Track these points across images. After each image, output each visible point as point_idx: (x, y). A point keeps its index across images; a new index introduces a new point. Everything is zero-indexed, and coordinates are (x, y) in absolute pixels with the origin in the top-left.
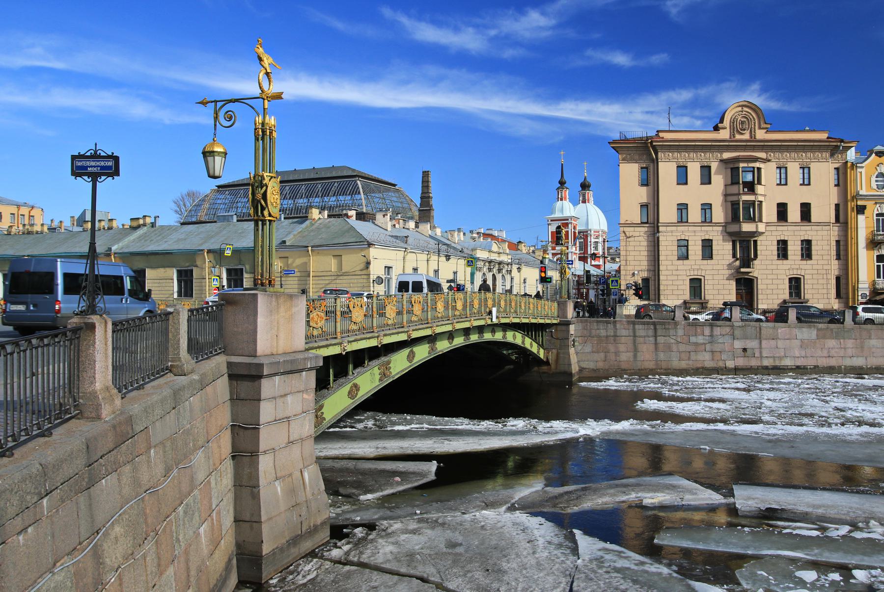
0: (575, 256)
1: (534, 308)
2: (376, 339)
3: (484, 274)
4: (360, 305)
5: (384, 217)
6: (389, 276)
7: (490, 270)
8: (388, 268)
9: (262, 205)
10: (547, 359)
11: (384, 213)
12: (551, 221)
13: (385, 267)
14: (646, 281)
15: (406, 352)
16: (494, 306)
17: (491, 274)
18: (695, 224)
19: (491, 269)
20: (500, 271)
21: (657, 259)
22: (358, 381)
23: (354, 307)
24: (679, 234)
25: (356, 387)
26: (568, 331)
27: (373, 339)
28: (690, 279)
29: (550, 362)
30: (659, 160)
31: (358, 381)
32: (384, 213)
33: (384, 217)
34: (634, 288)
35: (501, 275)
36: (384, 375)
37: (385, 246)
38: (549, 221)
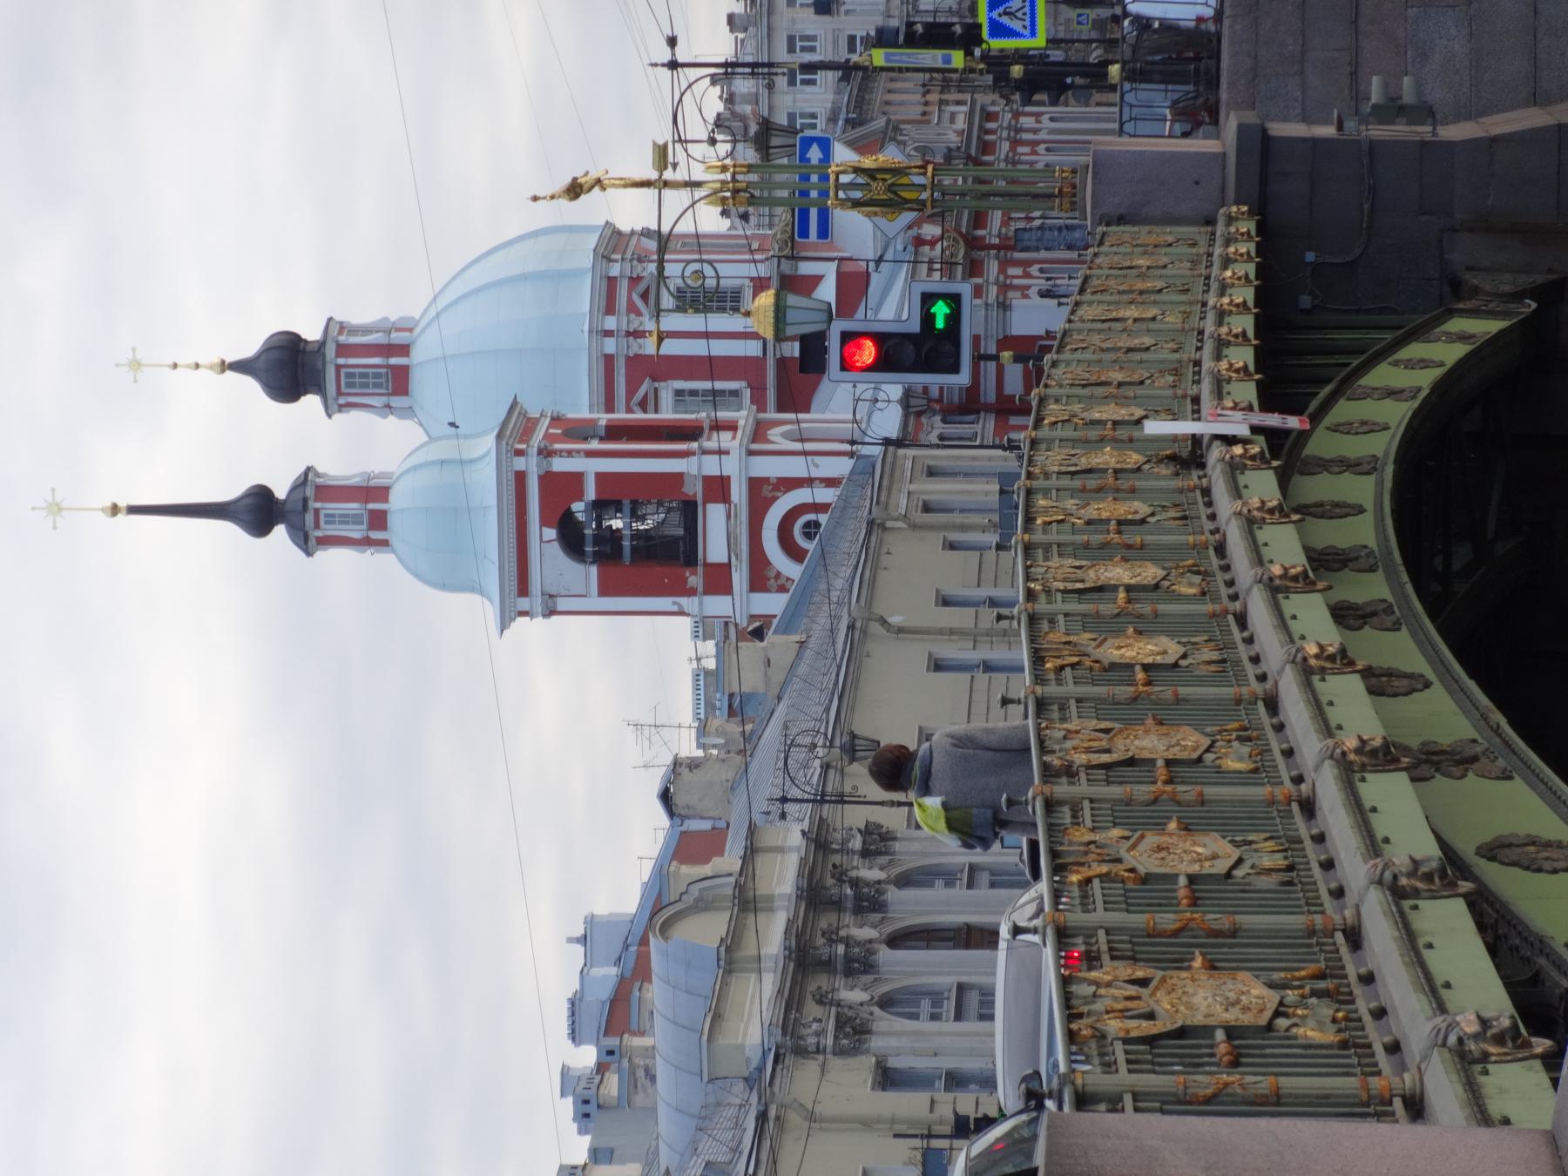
0: (774, 434)
3: (886, 1003)
4: (1132, 990)
7: (859, 965)
10: (1518, 296)
12: (523, 590)
17: (885, 954)
19: (848, 959)
20: (869, 903)
23: (1150, 1016)
29: (1540, 279)
35: (893, 894)
38: (524, 603)
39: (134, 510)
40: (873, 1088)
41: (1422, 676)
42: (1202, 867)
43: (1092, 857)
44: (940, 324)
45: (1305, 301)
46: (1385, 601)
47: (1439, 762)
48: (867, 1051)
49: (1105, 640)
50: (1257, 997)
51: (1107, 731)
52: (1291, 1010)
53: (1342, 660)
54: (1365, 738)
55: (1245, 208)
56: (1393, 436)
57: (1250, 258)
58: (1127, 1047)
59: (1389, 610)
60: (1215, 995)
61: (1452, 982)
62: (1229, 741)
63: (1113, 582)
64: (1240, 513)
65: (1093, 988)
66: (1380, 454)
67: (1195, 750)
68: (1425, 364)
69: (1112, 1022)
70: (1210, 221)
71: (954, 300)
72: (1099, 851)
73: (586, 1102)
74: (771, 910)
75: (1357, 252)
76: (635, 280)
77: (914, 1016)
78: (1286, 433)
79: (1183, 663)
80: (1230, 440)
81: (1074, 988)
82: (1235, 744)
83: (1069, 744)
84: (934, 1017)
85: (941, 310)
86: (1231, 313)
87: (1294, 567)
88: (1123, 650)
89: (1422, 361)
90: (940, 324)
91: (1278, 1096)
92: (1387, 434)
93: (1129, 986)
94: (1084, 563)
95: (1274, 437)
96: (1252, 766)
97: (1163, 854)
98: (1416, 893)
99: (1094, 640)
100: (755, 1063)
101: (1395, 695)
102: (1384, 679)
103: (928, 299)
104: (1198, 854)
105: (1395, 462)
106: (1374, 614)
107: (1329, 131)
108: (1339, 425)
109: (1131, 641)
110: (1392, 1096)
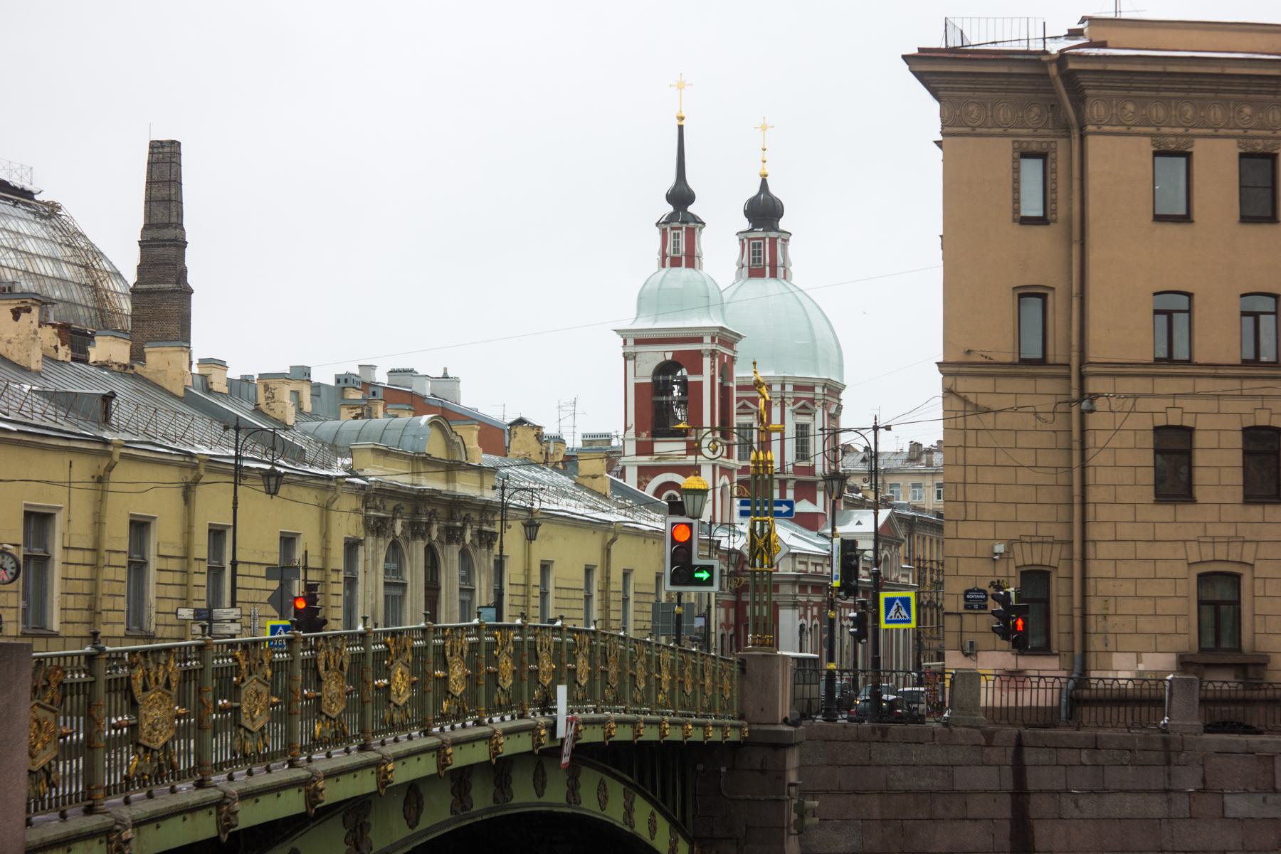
0: (725, 480)
1: (672, 683)
3: (395, 545)
6: (38, 551)
7: (416, 530)
11: (15, 304)
12: (638, 342)
14: (1036, 578)
16: (558, 679)
18: (1215, 370)
19: (419, 524)
20: (452, 535)
21: (1077, 500)
23: (145, 689)
24: (1158, 405)
26: (781, 773)
27: (206, 812)
28: (1200, 576)
30: (1090, 128)
34: (993, 605)
38: (631, 342)
39: (681, 128)
40: (346, 538)
41: (417, 824)
42: (246, 713)
43: (253, 662)
44: (697, 575)
45: (700, 767)
46: (472, 807)
47: (355, 831)
48: (366, 535)
49: (408, 667)
50: (157, 739)
51: (341, 667)
52: (149, 754)
53: (384, 780)
54: (323, 792)
55: (746, 735)
56: (599, 814)
57: (706, 738)
58: (125, 679)
59: (464, 808)
60: (158, 719)
61: (160, 829)
62: (335, 727)
63: (451, 670)
64: (495, 733)
65: (163, 662)
66: (581, 806)
67: (329, 710)
68: (653, 830)
69: (141, 671)
70: (742, 717)
71: (709, 582)
72: (257, 665)
73: (346, 381)
74: (448, 481)
75: (726, 794)
76: (812, 401)
77: (387, 560)
78: (560, 757)
79: (392, 705)
81: (163, 654)
82: (333, 730)
83: (332, 650)
84: (386, 571)
85: (705, 575)
86: (635, 728)
87: (451, 759)
88: (400, 676)
89: (655, 828)
90: (697, 575)
91: (93, 748)
92: (600, 811)
93: (165, 678)
94: (552, 652)
95: (556, 752)
96: (317, 738)
97: (254, 695)
98: (219, 814)
99: (408, 661)
100: (360, 473)
101: (404, 811)
102: (415, 805)
103: (710, 569)
104: (255, 712)
105: (573, 814)
106: (462, 801)
107: (792, 777)
108: (605, 785)
109: (407, 679)
110: (94, 800)
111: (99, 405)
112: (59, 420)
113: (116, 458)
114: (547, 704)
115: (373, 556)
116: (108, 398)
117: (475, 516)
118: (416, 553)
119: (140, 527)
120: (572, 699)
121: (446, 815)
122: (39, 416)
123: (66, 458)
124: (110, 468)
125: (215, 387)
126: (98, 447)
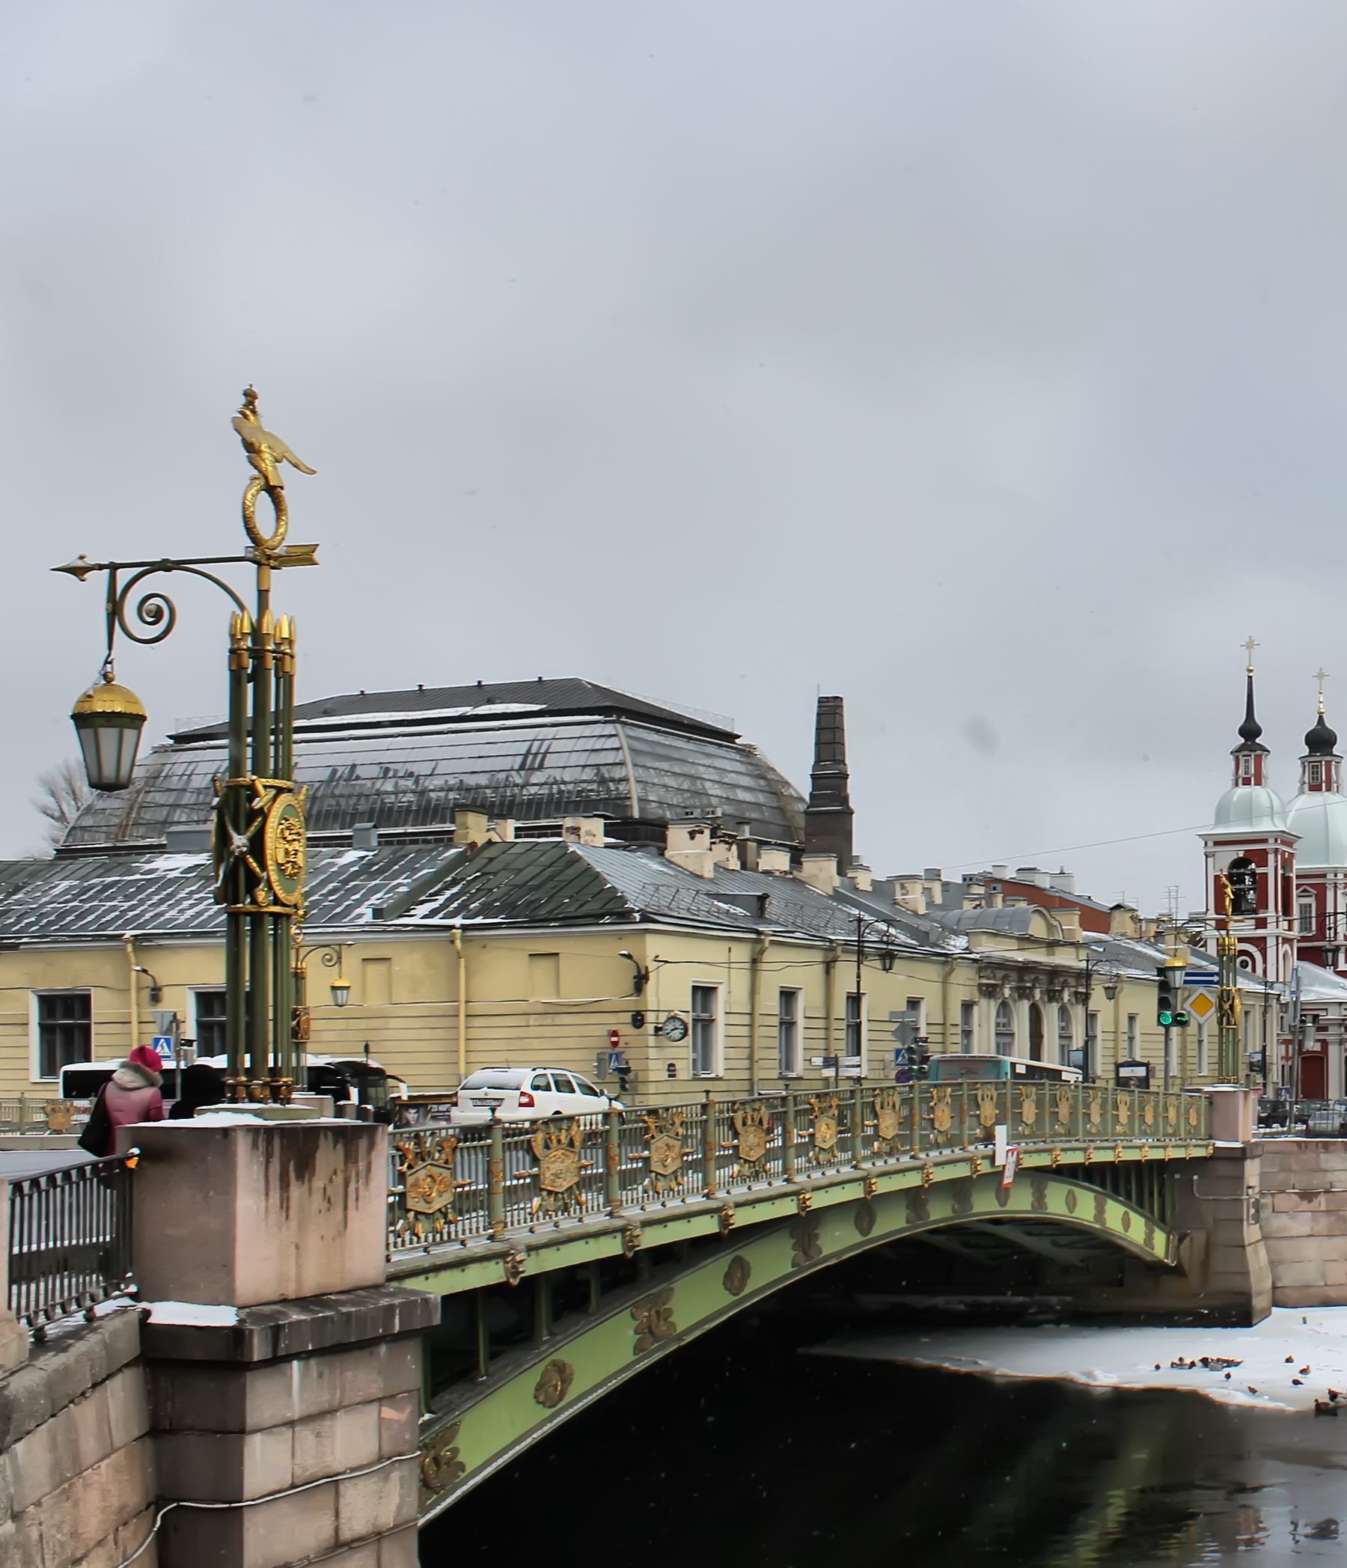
0: (1287, 947)
2: (619, 1236)
3: (1004, 1005)
5: (692, 838)
6: (705, 1016)
8: (704, 994)
9: (250, 872)
11: (691, 827)
13: (695, 989)
15: (717, 1267)
16: (999, 1121)
22: (560, 1355)
25: (563, 1372)
31: (560, 1355)
32: (691, 827)
33: (692, 838)
36: (648, 1333)
37: (696, 928)
77: (998, 1016)
80: (992, 1158)
84: (998, 1025)
111: (755, 903)
112: (720, 916)
113: (767, 945)
114: (989, 1138)
115: (986, 1012)
116: (762, 899)
117: (1072, 981)
118: (1022, 1012)
119: (788, 996)
120: (1013, 1138)
121: (903, 1224)
122: (706, 914)
123: (726, 945)
124: (762, 952)
125: (861, 887)
126: (753, 936)
